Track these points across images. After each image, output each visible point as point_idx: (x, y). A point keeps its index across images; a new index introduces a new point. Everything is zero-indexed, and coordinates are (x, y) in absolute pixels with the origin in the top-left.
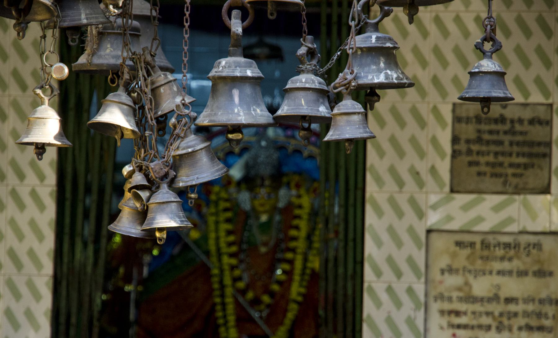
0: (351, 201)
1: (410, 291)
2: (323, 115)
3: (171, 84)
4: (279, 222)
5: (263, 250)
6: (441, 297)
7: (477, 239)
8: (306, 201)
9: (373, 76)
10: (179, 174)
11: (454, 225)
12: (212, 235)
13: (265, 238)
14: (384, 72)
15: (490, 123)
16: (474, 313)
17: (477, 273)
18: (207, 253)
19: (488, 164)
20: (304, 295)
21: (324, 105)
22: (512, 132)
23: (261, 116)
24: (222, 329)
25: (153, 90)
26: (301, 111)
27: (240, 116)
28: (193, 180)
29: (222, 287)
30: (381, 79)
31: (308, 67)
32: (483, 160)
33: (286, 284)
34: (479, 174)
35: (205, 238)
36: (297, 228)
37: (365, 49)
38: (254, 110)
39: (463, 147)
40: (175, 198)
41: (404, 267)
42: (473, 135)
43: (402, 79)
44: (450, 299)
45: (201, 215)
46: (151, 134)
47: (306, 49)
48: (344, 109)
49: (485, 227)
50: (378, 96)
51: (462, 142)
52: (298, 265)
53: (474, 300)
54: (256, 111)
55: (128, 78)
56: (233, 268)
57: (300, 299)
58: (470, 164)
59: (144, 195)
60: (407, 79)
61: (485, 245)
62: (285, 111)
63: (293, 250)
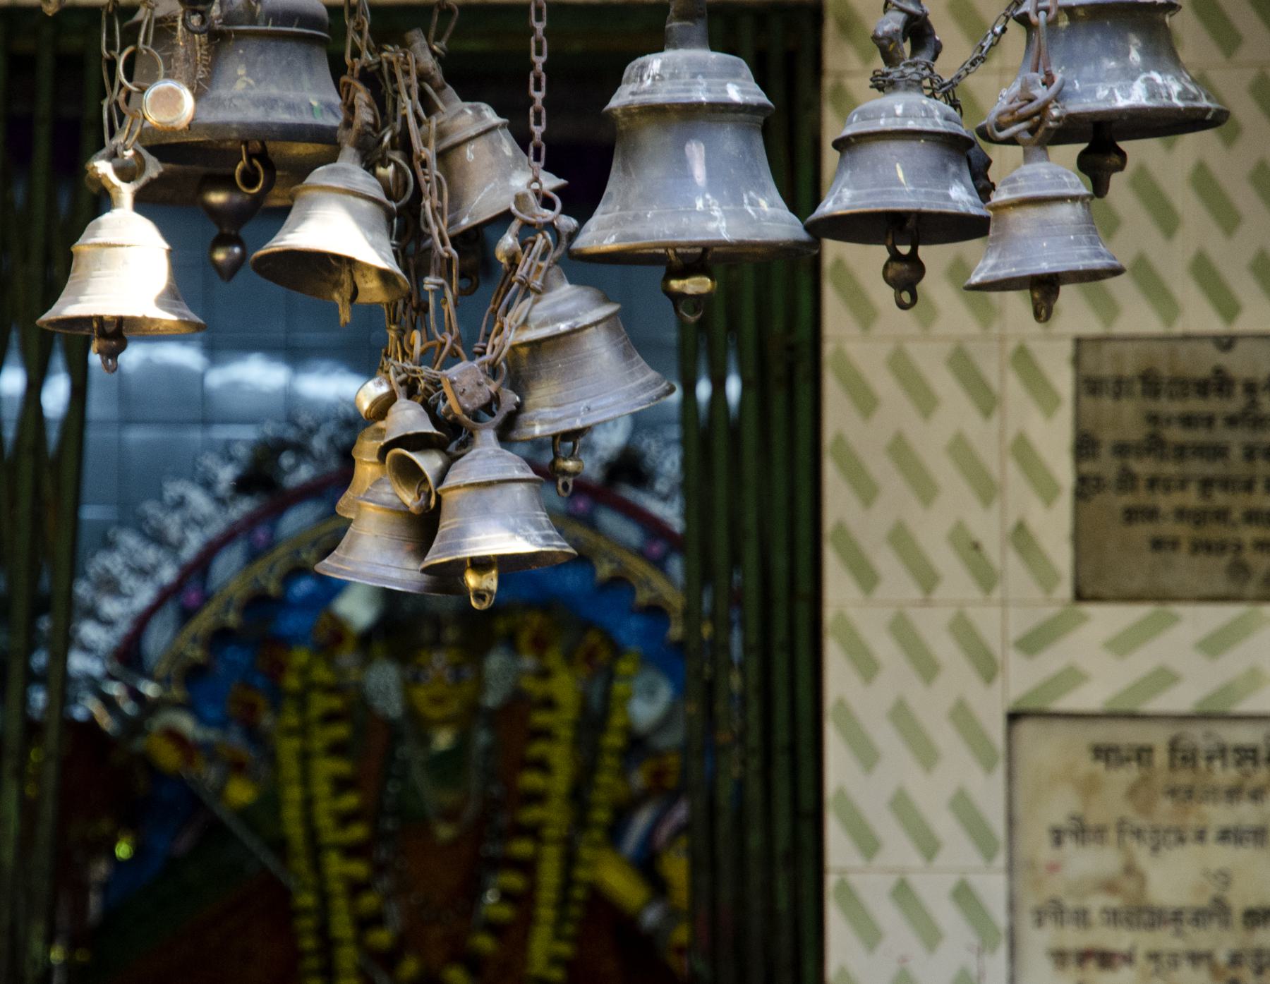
0: (780, 634)
1: (964, 895)
2: (962, 209)
3: (493, 135)
5: (445, 832)
6: (1053, 912)
7: (1158, 737)
9: (1111, 90)
10: (529, 402)
11: (1089, 698)
12: (294, 794)
13: (448, 798)
14: (1143, 76)
15: (1186, 395)
16: (1154, 956)
17: (1159, 839)
18: (280, 847)
19: (1181, 514)
21: (962, 182)
22: (1251, 418)
23: (774, 219)
25: (442, 156)
26: (895, 199)
27: (713, 219)
28: (576, 415)
30: (1134, 96)
31: (909, 71)
32: (1166, 502)
33: (513, 935)
34: (1158, 544)
35: (270, 802)
36: (542, 766)
37: (1081, 13)
38: (753, 203)
39: (1106, 466)
40: (523, 469)
41: (945, 825)
42: (1135, 432)
43: (1195, 99)
44: (1082, 918)
45: (254, 735)
46: (442, 286)
47: (901, 17)
48: (1030, 188)
49: (1180, 699)
50: (1122, 155)
51: (1105, 451)
52: (549, 874)
53: (1153, 917)
54: (758, 205)
55: (370, 119)
56: (356, 888)
58: (1131, 515)
59: (429, 463)
60: (1208, 98)
61: (1181, 755)
62: (846, 201)
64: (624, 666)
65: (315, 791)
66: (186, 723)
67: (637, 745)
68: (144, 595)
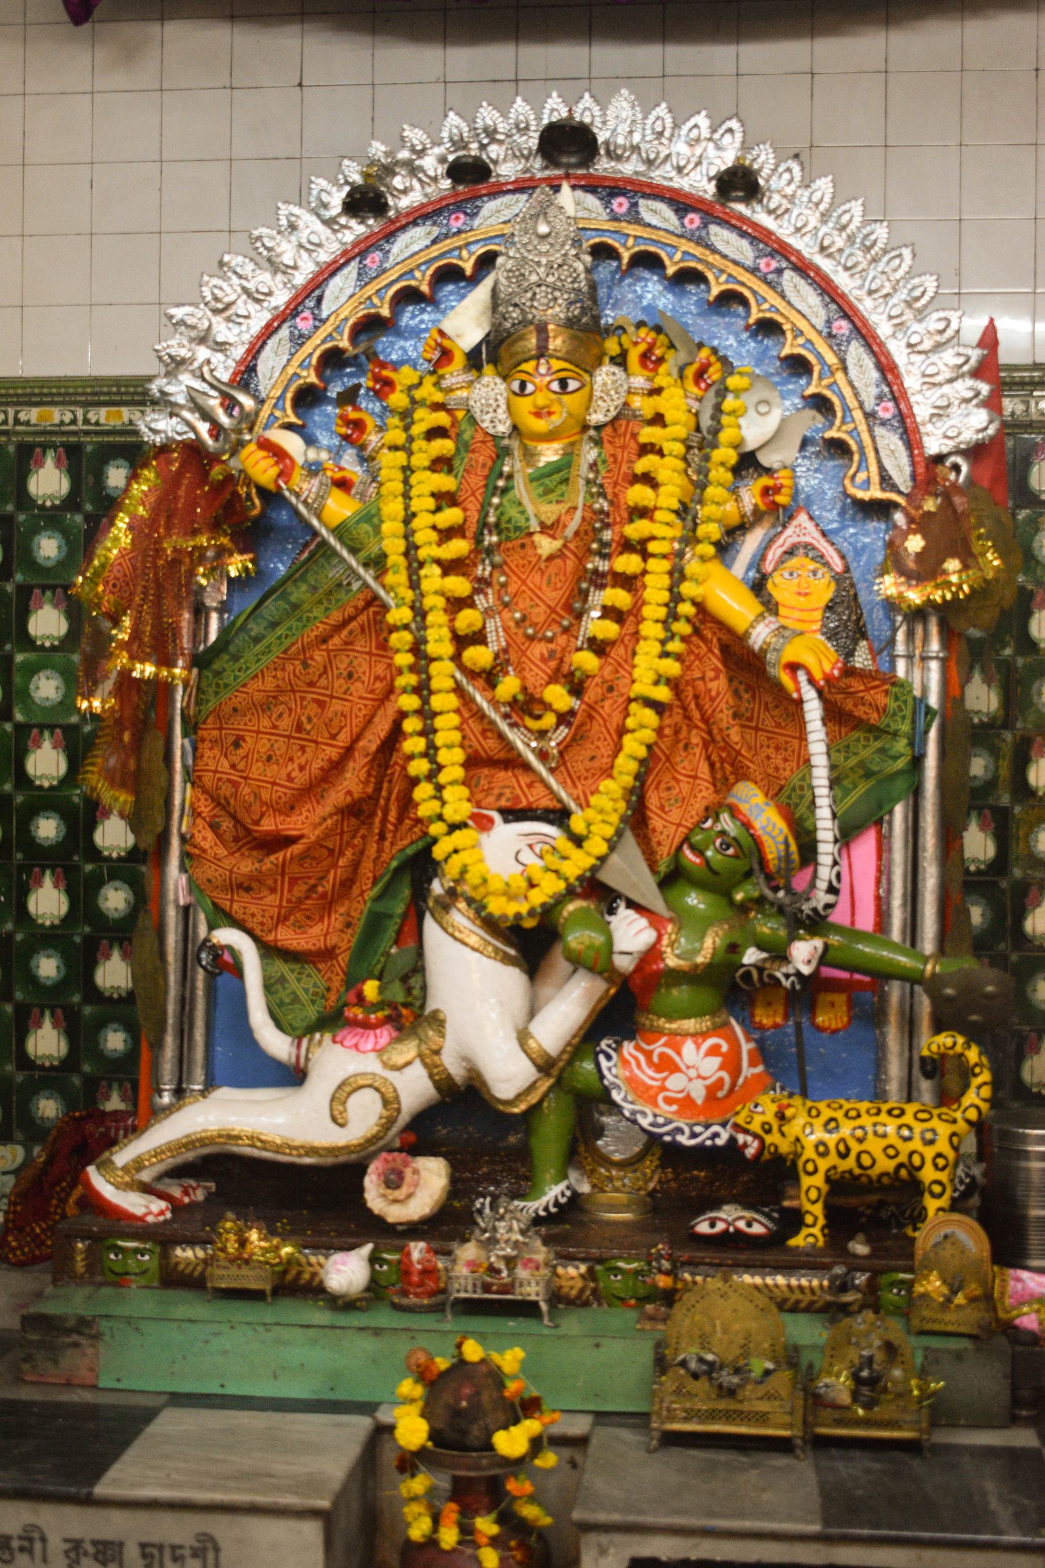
4: (593, 466)
5: (546, 545)
8: (677, 403)
18: (378, 563)
20: (673, 684)
24: (423, 791)
35: (372, 518)
36: (648, 479)
52: (656, 590)
56: (456, 604)
57: (663, 694)
63: (640, 548)
64: (733, 382)
66: (292, 443)
67: (747, 463)
68: (259, 319)
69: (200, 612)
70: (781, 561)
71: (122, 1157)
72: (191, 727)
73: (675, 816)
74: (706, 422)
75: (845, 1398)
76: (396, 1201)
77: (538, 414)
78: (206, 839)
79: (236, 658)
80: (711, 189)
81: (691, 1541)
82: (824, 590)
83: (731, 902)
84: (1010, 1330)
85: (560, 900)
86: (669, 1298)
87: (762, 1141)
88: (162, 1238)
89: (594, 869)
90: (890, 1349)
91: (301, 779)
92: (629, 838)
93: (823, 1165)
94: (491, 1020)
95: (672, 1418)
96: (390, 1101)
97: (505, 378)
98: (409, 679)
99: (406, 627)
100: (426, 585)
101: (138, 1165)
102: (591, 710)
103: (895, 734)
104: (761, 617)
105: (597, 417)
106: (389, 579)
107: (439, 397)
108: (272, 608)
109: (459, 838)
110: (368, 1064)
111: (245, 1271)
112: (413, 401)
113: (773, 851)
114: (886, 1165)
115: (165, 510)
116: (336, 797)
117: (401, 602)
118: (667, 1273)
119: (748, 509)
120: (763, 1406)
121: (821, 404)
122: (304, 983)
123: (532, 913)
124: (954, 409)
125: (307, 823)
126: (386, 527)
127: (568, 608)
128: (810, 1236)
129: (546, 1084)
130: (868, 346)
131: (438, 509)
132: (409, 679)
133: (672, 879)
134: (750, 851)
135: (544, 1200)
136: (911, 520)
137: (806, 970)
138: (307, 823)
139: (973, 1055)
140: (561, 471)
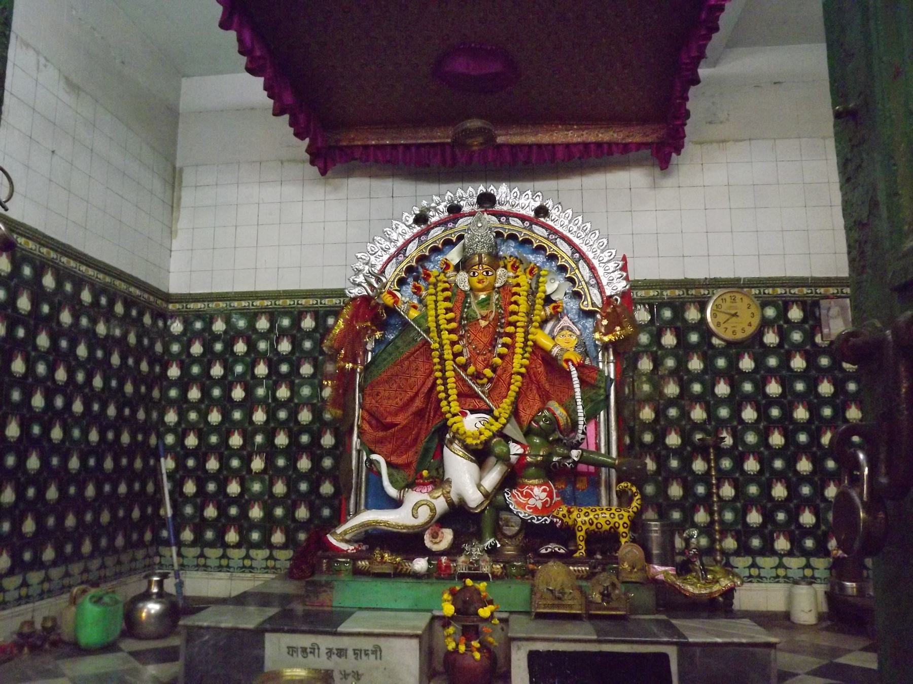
4: (497, 299)
5: (483, 323)
8: (524, 279)
18: (428, 331)
20: (526, 367)
24: (444, 403)
29: (442, 360)
35: (425, 316)
52: (520, 337)
56: (453, 343)
57: (523, 370)
63: (514, 324)
64: (542, 273)
65: (438, 312)
67: (548, 300)
68: (386, 257)
69: (366, 352)
70: (559, 332)
71: (339, 531)
72: (362, 390)
73: (528, 412)
74: (534, 286)
75: (600, 601)
76: (436, 543)
77: (479, 282)
78: (366, 427)
79: (377, 366)
80: (532, 214)
81: (551, 644)
82: (574, 340)
83: (548, 441)
84: (654, 581)
85: (490, 439)
86: (533, 573)
87: (562, 520)
88: (354, 558)
89: (502, 428)
90: (613, 585)
91: (401, 403)
92: (513, 420)
93: (584, 528)
94: (466, 480)
95: (539, 607)
96: (433, 510)
97: (467, 272)
98: (438, 367)
99: (437, 350)
100: (443, 337)
101: (345, 533)
102: (499, 377)
103: (600, 388)
104: (555, 345)
105: (497, 285)
106: (431, 335)
107: (446, 279)
108: (389, 348)
109: (456, 419)
110: (426, 497)
111: (384, 566)
112: (437, 281)
113: (562, 422)
114: (608, 527)
115: (355, 316)
116: (413, 408)
117: (435, 342)
118: (533, 564)
119: (549, 313)
120: (570, 602)
121: (571, 280)
122: (400, 476)
123: (481, 443)
124: (615, 281)
125: (401, 419)
126: (430, 319)
127: (491, 344)
128: (581, 552)
129: (487, 502)
130: (585, 262)
131: (446, 313)
132: (438, 367)
133: (528, 433)
134: (554, 420)
135: (486, 545)
136: (602, 316)
137: (576, 459)
138: (401, 419)
139: (634, 489)
140: (485, 303)
